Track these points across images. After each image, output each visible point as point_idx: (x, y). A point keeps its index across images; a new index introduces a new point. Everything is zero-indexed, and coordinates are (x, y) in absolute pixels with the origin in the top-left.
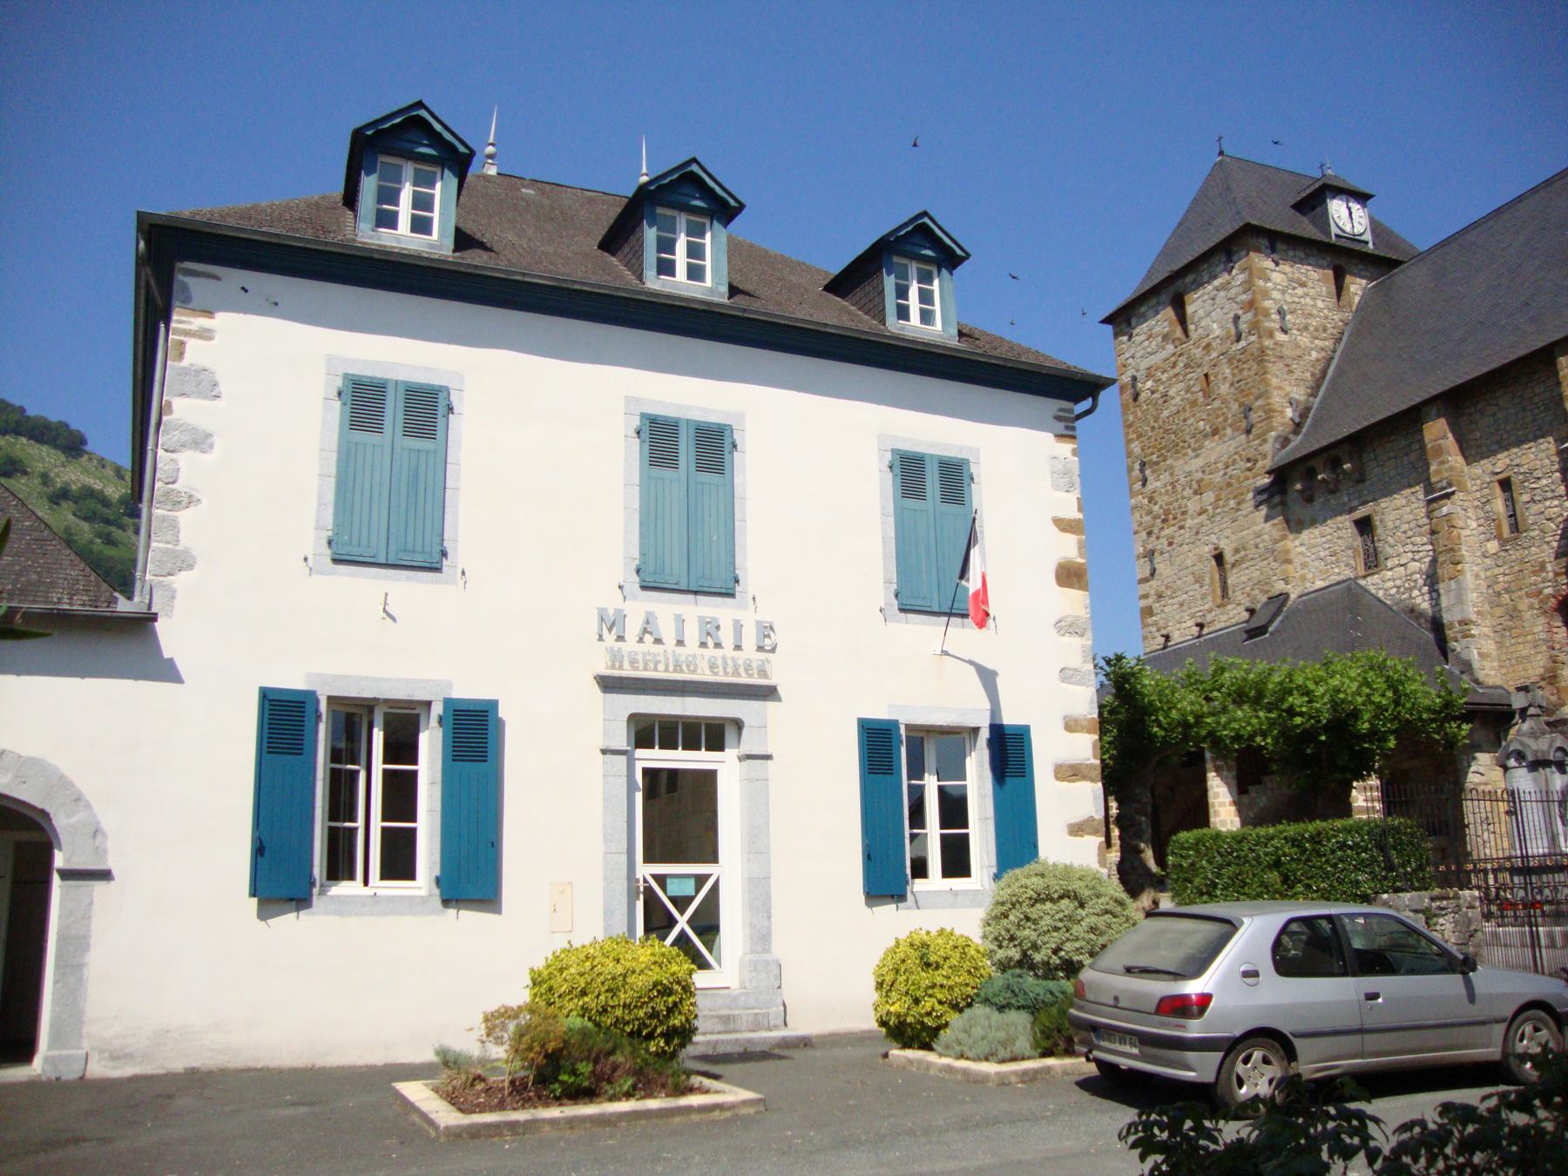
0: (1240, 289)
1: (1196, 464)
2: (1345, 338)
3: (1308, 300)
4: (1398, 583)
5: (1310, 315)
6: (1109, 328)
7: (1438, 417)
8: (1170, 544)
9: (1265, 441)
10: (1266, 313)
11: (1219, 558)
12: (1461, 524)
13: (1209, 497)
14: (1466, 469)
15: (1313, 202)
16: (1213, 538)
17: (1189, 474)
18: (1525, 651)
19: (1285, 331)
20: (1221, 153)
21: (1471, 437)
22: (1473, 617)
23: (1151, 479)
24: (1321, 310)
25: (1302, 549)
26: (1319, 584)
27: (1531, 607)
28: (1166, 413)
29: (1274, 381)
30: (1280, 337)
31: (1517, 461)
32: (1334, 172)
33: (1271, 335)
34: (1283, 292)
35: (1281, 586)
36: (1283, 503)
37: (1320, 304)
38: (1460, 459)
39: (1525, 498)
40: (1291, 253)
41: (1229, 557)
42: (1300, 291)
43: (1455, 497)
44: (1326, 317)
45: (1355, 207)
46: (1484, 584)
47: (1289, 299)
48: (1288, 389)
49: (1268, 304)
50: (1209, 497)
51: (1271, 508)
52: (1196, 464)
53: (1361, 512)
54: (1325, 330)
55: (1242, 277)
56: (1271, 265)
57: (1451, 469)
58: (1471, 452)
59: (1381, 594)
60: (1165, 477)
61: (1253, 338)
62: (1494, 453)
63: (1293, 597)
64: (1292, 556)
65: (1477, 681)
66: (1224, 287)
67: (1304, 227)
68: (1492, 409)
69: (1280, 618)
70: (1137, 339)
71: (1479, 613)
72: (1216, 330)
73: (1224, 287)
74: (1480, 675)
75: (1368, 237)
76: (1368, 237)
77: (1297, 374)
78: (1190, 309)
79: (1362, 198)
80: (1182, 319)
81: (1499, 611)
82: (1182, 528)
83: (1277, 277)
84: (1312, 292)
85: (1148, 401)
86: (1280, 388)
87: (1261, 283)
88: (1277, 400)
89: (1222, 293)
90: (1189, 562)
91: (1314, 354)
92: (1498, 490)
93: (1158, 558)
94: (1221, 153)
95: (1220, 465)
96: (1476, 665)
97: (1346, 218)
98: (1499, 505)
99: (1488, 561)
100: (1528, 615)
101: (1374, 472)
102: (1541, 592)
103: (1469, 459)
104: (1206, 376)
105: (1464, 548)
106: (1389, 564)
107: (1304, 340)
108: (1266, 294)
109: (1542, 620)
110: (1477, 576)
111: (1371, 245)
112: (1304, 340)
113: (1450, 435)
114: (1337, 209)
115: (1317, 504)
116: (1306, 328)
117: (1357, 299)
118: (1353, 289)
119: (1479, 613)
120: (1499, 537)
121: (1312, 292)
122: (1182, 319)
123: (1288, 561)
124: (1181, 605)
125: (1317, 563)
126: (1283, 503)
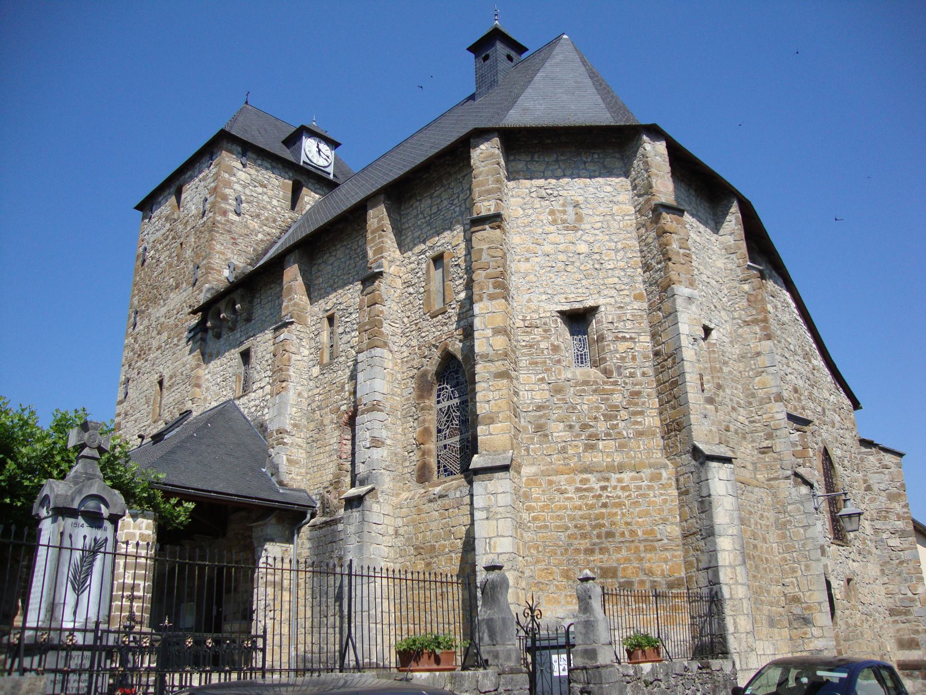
0: (212, 180)
1: (164, 310)
2: (291, 231)
3: (265, 197)
4: (257, 402)
5: (265, 208)
6: (140, 213)
7: (294, 263)
8: (139, 373)
9: (201, 291)
10: (225, 198)
11: (161, 383)
12: (293, 349)
13: (165, 336)
14: (309, 307)
15: (293, 140)
16: (161, 368)
17: (158, 319)
18: (323, 459)
19: (239, 215)
20: (246, 103)
21: (317, 282)
22: (289, 428)
23: (138, 324)
24: (275, 207)
25: (209, 376)
26: (214, 404)
27: (332, 422)
28: (155, 274)
29: (218, 247)
30: (233, 217)
31: (340, 300)
32: (314, 125)
33: (225, 213)
34: (244, 187)
35: (189, 405)
36: (203, 340)
37: (275, 202)
38: (305, 298)
39: (341, 330)
40: (259, 162)
41: (166, 384)
42: (260, 190)
43: (293, 327)
44: (278, 213)
45: (324, 147)
46: (305, 403)
47: (248, 192)
48: (230, 255)
49: (227, 191)
50: (165, 336)
51: (195, 343)
52: (164, 310)
53: (243, 348)
54: (275, 221)
55: (214, 171)
56: (240, 166)
57: (295, 304)
58: (313, 292)
59: (246, 412)
60: (146, 322)
61: (211, 214)
62: (328, 294)
63: (194, 414)
64: (202, 381)
65: (281, 483)
66: (204, 179)
67: (287, 154)
68: (332, 259)
69: (177, 429)
70: (153, 220)
71: (295, 425)
72: (194, 211)
73: (204, 179)
74: (286, 479)
75: (330, 170)
76: (330, 170)
77: (242, 246)
78: (183, 196)
79: (334, 144)
80: (179, 201)
81: (312, 426)
82: (146, 361)
83: (242, 175)
84: (270, 193)
85: (149, 266)
86: (223, 254)
87: (226, 176)
88: (216, 261)
89: (202, 183)
90: (145, 388)
91: (260, 236)
92: (326, 321)
93: (131, 384)
94: (246, 103)
95: (175, 312)
96: (283, 468)
97: (313, 152)
98: (325, 337)
99: (311, 383)
100: (328, 429)
101: (258, 313)
102: (339, 409)
103: (312, 300)
104: (181, 244)
105: (292, 369)
106: (255, 387)
107: (254, 224)
108: (228, 184)
109: (337, 433)
110: (299, 394)
111: (331, 177)
112: (254, 224)
113: (300, 279)
114: (309, 145)
115: (222, 340)
116: (258, 216)
117: (308, 207)
118: (306, 199)
119: (295, 425)
120: (320, 363)
121: (270, 193)
122: (179, 201)
123: (198, 386)
124: (136, 421)
125: (214, 388)
126: (203, 340)
